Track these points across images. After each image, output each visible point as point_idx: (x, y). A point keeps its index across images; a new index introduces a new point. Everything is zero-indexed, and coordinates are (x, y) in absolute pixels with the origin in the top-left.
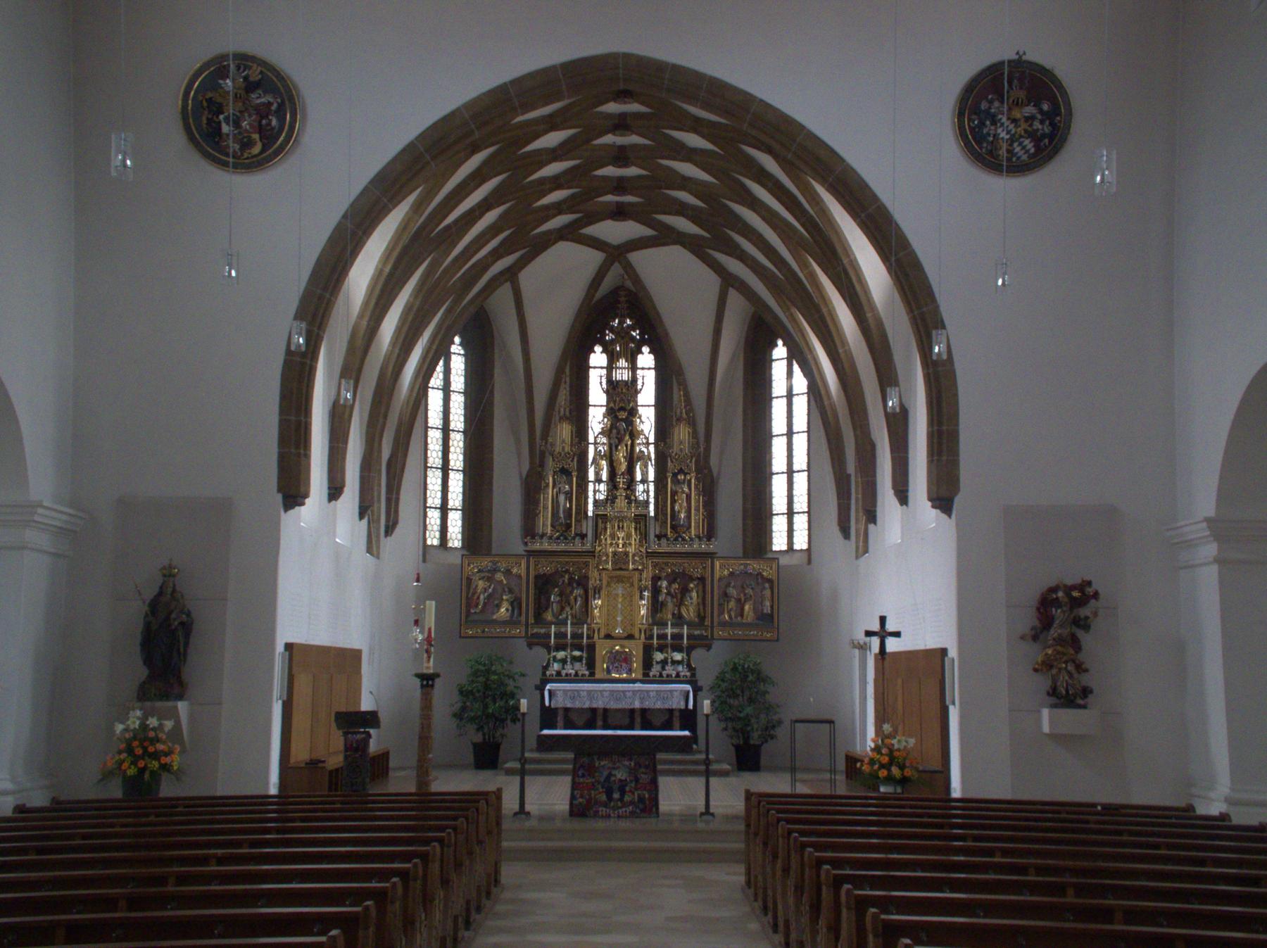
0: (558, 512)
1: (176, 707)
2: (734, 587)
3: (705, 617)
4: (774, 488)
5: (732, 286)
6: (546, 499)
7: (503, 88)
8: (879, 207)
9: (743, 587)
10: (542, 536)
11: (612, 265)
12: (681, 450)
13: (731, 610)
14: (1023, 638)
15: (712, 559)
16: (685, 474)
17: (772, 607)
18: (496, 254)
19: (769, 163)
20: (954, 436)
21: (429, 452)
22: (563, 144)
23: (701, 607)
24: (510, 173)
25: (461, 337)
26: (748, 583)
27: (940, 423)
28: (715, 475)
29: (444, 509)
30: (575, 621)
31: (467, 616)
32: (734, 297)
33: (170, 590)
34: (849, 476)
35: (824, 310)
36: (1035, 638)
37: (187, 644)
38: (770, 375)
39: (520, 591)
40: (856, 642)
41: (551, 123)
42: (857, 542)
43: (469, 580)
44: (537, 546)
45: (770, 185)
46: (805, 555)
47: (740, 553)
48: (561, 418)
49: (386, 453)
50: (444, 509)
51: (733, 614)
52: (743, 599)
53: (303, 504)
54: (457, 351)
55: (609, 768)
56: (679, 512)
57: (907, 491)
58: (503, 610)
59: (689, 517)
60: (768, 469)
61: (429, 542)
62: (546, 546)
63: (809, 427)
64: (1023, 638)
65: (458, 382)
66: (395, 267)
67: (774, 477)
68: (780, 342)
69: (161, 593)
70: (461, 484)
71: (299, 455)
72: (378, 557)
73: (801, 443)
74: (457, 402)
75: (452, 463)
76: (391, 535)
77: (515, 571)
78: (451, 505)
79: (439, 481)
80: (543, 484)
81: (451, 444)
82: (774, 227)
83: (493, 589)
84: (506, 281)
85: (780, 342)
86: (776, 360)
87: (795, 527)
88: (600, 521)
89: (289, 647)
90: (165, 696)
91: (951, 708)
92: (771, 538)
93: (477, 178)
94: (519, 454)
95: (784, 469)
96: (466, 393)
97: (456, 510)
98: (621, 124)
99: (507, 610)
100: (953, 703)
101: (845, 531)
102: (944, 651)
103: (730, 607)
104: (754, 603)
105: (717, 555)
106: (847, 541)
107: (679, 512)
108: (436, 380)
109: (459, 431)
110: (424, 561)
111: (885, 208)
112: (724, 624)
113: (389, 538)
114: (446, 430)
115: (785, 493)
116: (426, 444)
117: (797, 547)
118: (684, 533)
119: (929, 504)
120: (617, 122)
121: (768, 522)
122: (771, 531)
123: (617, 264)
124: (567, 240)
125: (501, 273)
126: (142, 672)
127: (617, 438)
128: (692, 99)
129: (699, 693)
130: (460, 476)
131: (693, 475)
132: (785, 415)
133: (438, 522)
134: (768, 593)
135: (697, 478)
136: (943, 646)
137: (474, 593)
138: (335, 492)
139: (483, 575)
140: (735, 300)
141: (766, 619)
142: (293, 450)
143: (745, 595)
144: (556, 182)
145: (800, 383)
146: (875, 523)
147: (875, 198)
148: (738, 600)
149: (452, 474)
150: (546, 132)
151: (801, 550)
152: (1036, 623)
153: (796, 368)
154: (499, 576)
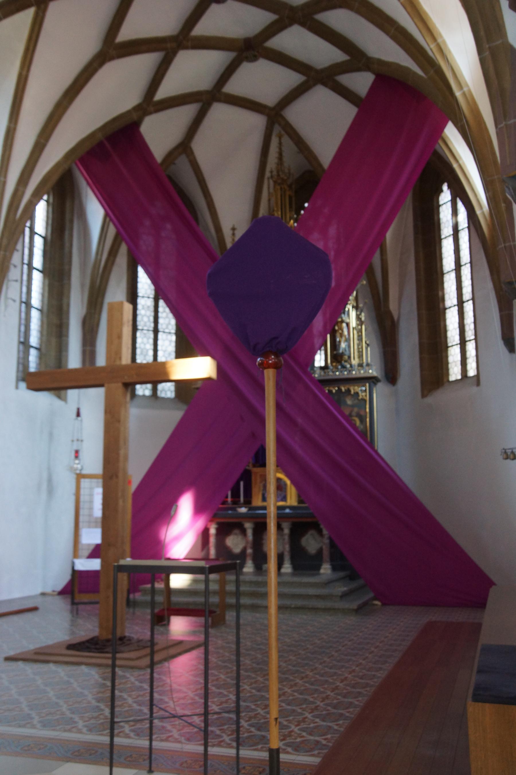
28: (396, 317)
38: (439, 219)
46: (475, 378)
60: (441, 306)
68: (445, 187)
70: (173, 344)
79: (151, 341)
85: (445, 187)
86: (443, 205)
92: (447, 369)
95: (455, 302)
115: (456, 325)
118: (346, 361)
121: (444, 354)
122: (447, 363)
124: (219, 100)
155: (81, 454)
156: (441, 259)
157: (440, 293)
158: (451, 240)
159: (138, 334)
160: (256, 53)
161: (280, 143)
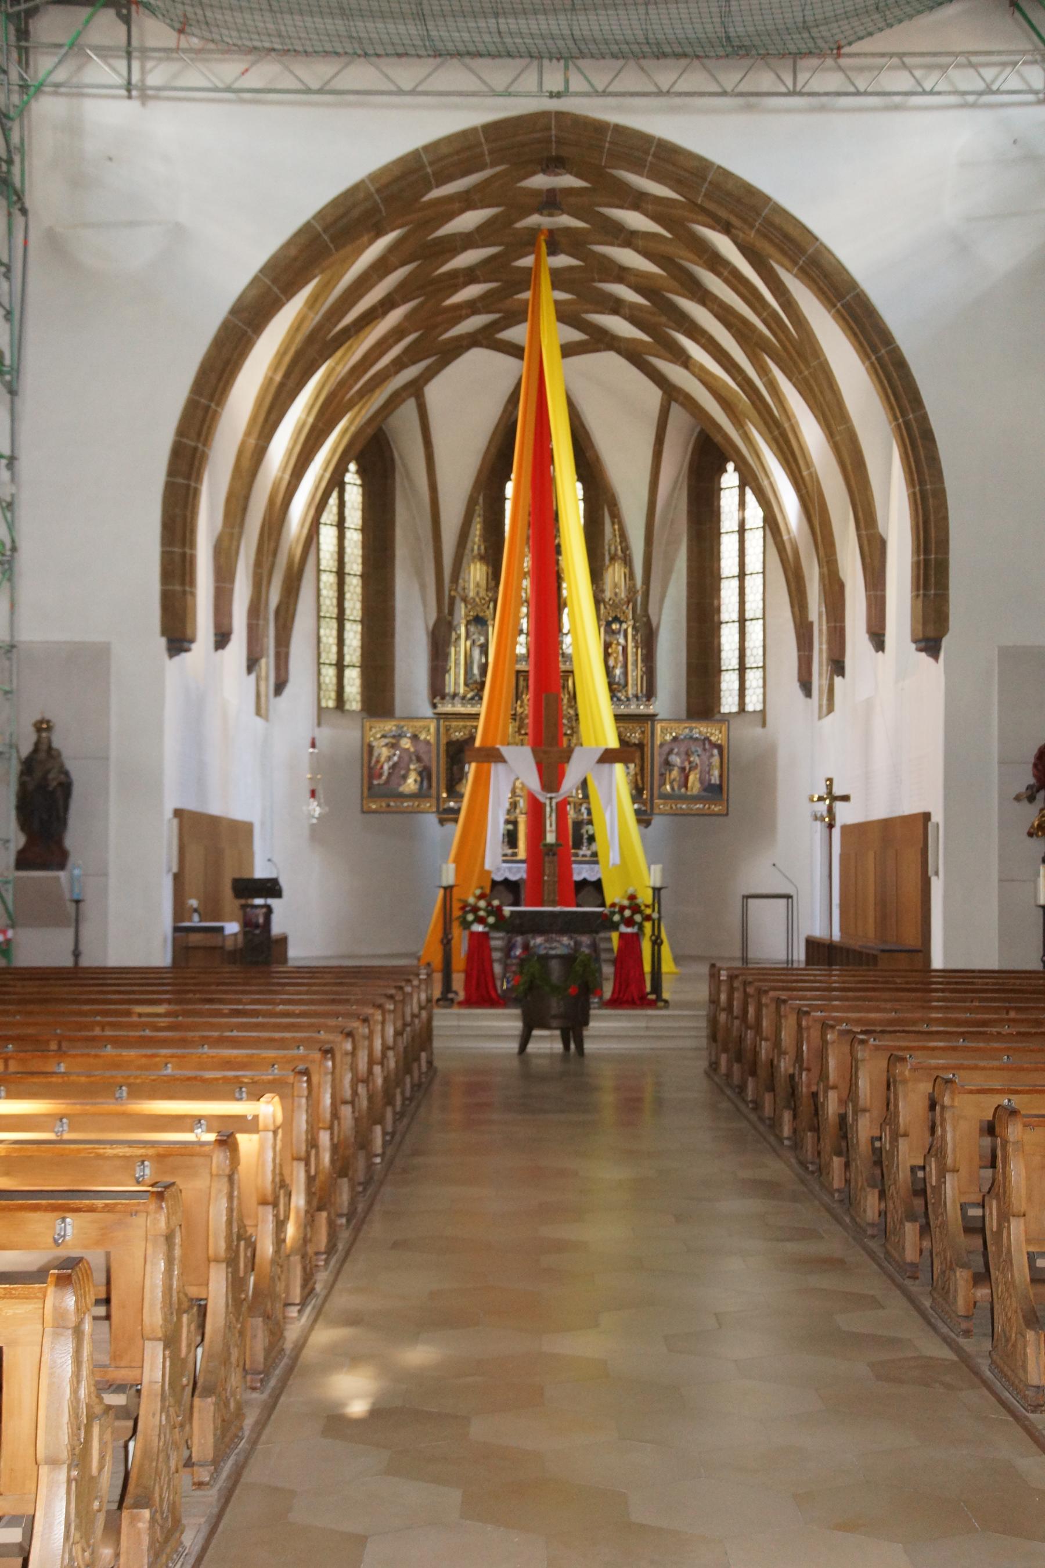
0: (472, 668)
1: (58, 879)
2: (677, 754)
3: (643, 789)
4: (724, 640)
5: (676, 401)
6: (457, 653)
7: (415, 154)
8: (858, 295)
9: (688, 754)
12: (616, 594)
13: (674, 780)
14: (1018, 798)
15: (653, 721)
16: (621, 623)
17: (721, 776)
18: (399, 365)
19: (724, 245)
20: (942, 567)
21: (322, 599)
22: (480, 229)
23: (639, 778)
24: (419, 262)
25: (359, 464)
26: (693, 749)
27: (927, 551)
28: (654, 625)
29: (340, 666)
31: (371, 787)
32: (677, 412)
33: (44, 747)
34: (811, 624)
35: (786, 425)
36: (1031, 799)
37: (66, 808)
38: (719, 507)
39: (430, 760)
40: (819, 815)
41: (466, 201)
42: (820, 699)
43: (371, 748)
44: (447, 708)
45: (726, 273)
46: (759, 717)
47: (683, 714)
48: (474, 557)
50: (340, 666)
51: (676, 787)
52: (687, 768)
53: (188, 650)
54: (352, 481)
55: (545, 948)
56: (614, 667)
57: (884, 635)
58: (410, 781)
59: (625, 673)
60: (716, 617)
61: (324, 704)
62: (460, 709)
63: (764, 567)
64: (1018, 798)
65: (354, 517)
66: (287, 375)
67: (723, 626)
69: (36, 749)
70: (359, 637)
71: (184, 592)
72: (267, 719)
73: (754, 586)
74: (354, 538)
75: (348, 612)
77: (422, 736)
78: (347, 659)
79: (335, 633)
80: (454, 636)
81: (346, 588)
82: (728, 326)
83: (400, 757)
84: (410, 396)
85: (730, 466)
87: (748, 684)
88: (521, 679)
89: (178, 813)
90: (44, 866)
91: (934, 880)
92: (719, 698)
93: (381, 268)
94: (425, 604)
95: (735, 616)
96: (364, 530)
97: (354, 666)
98: (551, 201)
99: (415, 781)
100: (937, 874)
101: (806, 687)
102: (926, 816)
103: (672, 776)
104: (701, 773)
105: (658, 717)
106: (808, 700)
107: (614, 667)
108: (330, 515)
109: (355, 575)
110: (319, 724)
111: (865, 295)
112: (665, 797)
113: (278, 699)
114: (341, 574)
115: (737, 646)
116: (318, 590)
117: (750, 708)
119: (914, 646)
122: (720, 690)
125: (406, 387)
126: (19, 840)
128: (637, 167)
130: (358, 628)
131: (631, 623)
132: (737, 553)
133: (334, 680)
134: (716, 760)
135: (634, 628)
136: (926, 810)
137: (378, 761)
138: (222, 639)
139: (386, 741)
140: (678, 414)
141: (715, 791)
142: (178, 588)
143: (690, 763)
144: (470, 275)
145: (755, 514)
146: (843, 675)
147: (853, 285)
148: (683, 769)
149: (348, 626)
150: (463, 211)
151: (755, 712)
152: (1032, 781)
153: (750, 497)
154: (406, 743)
155: (317, 794)
156: (719, 560)
157: (716, 602)
158: (735, 537)
159: (323, 623)
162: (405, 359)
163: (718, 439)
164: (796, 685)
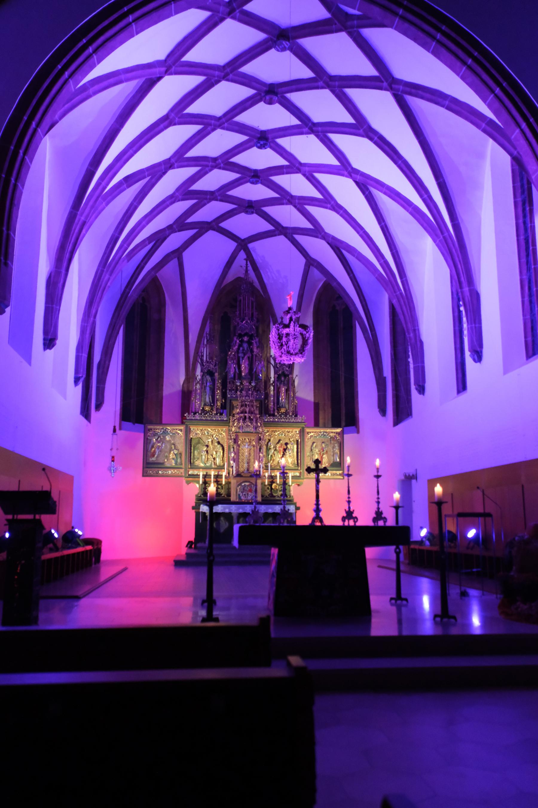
5: (313, 265)
10: (195, 413)
11: (240, 251)
30: (216, 467)
40: (407, 475)
49: (97, 358)
76: (99, 410)
84: (175, 258)
101: (383, 411)
106: (384, 417)
120: (267, 89)
123: (242, 251)
124: (214, 230)
127: (243, 353)
129: (298, 511)
146: (423, 394)
160: (254, 211)
161: (247, 264)
162: (175, 226)
163: (334, 284)
164: (377, 410)
